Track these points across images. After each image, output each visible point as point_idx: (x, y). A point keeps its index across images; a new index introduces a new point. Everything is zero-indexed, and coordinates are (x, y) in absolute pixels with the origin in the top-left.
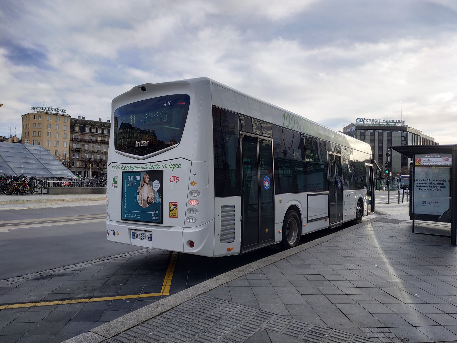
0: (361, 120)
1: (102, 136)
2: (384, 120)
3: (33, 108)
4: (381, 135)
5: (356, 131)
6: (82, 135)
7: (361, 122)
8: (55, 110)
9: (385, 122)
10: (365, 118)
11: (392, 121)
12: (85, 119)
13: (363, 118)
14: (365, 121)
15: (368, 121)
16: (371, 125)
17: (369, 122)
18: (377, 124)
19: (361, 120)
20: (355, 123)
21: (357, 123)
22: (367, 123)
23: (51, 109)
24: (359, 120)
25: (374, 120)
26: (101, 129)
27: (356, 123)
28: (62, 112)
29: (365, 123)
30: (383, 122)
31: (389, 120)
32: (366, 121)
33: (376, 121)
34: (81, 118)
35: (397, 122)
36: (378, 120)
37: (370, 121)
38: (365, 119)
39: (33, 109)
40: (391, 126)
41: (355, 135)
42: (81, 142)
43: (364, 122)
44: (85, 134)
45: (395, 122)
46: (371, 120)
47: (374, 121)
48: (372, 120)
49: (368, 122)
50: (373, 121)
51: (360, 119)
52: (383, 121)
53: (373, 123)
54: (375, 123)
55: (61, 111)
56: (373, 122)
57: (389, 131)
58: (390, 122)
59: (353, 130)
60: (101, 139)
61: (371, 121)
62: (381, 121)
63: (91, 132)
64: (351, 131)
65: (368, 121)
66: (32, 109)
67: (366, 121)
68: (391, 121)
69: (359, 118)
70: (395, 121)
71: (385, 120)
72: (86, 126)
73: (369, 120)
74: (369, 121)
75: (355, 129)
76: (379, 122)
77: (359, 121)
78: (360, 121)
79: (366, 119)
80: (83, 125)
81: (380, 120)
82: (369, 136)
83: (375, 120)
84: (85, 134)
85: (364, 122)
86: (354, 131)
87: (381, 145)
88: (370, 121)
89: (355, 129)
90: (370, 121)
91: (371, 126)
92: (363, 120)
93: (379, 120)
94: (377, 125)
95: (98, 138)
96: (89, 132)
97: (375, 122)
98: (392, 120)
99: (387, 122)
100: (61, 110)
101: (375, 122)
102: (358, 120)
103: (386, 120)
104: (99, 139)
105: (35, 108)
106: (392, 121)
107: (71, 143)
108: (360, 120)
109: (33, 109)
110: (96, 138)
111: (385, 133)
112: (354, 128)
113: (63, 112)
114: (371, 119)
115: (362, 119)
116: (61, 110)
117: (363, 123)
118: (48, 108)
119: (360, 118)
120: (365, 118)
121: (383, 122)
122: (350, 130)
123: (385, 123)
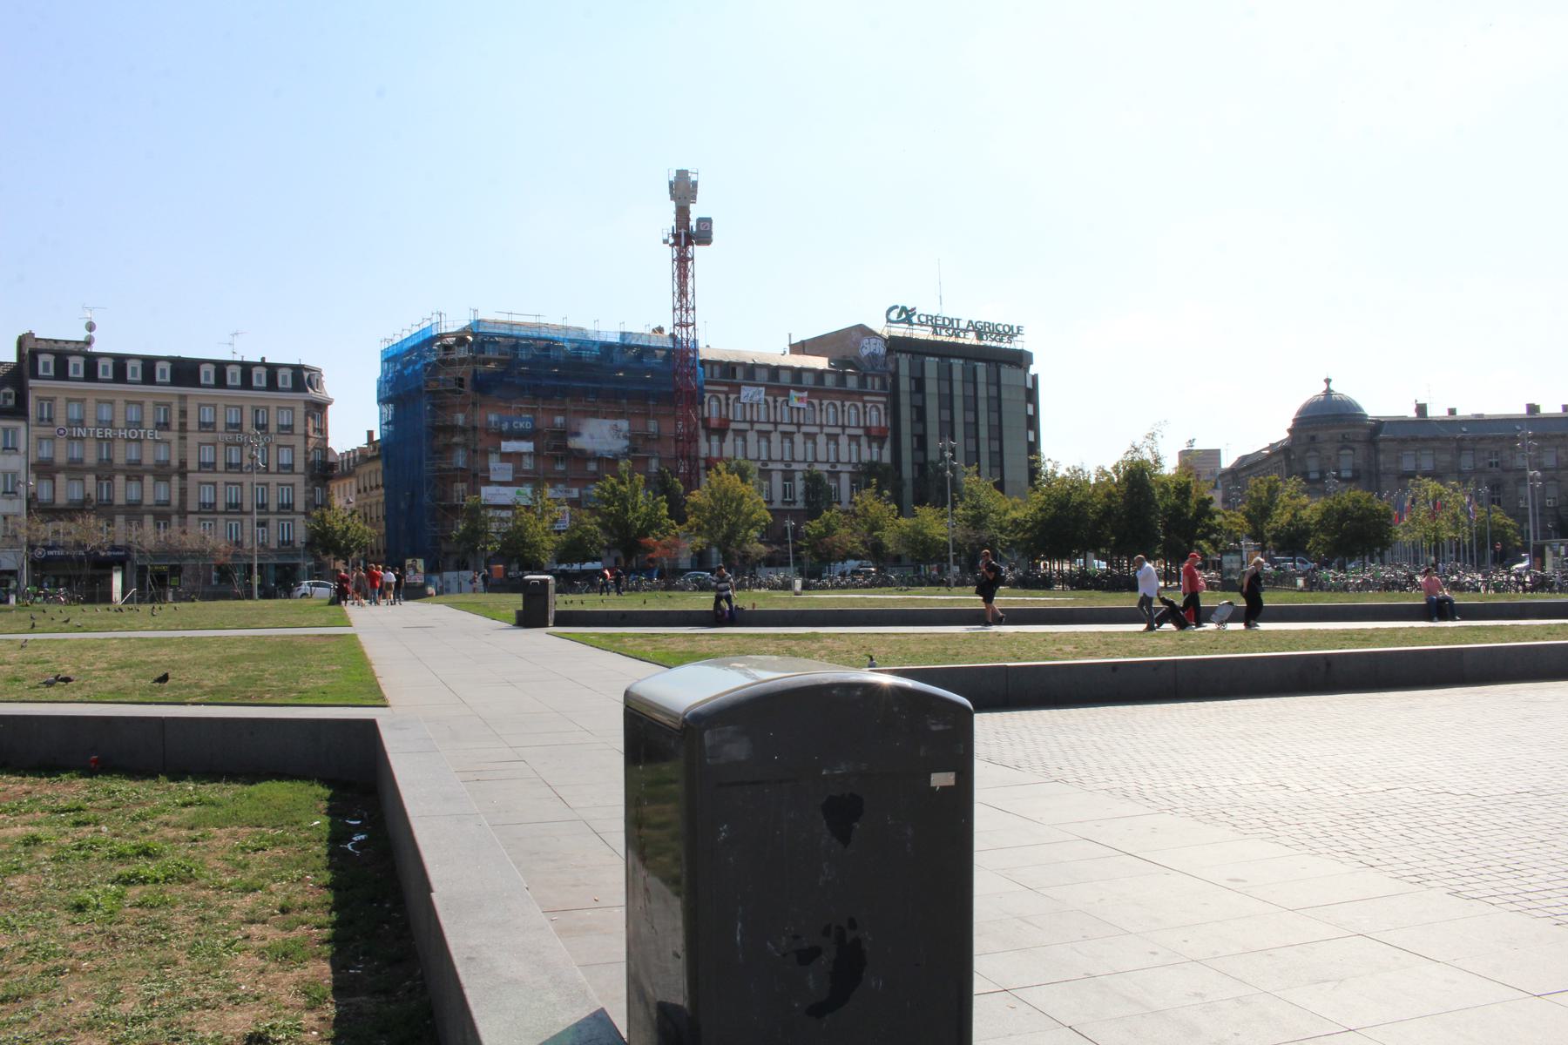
0: (904, 316)
7: (902, 321)
10: (915, 309)
11: (991, 328)
15: (923, 319)
19: (904, 316)
24: (896, 315)
29: (915, 327)
30: (966, 331)
31: (985, 323)
35: (1006, 334)
37: (931, 320)
38: (915, 314)
43: (911, 323)
45: (999, 333)
46: (932, 316)
47: (940, 322)
48: (936, 317)
49: (921, 324)
52: (968, 326)
54: (943, 332)
58: (987, 329)
61: (934, 321)
68: (989, 327)
69: (896, 307)
70: (1000, 328)
73: (927, 316)
74: (927, 320)
79: (918, 313)
81: (958, 320)
82: (936, 381)
83: (944, 318)
85: (911, 323)
88: (930, 323)
90: (930, 323)
92: (907, 315)
93: (955, 322)
102: (894, 316)
106: (991, 328)
108: (900, 315)
115: (904, 309)
117: (906, 326)
120: (915, 309)
121: (966, 331)
123: (970, 339)
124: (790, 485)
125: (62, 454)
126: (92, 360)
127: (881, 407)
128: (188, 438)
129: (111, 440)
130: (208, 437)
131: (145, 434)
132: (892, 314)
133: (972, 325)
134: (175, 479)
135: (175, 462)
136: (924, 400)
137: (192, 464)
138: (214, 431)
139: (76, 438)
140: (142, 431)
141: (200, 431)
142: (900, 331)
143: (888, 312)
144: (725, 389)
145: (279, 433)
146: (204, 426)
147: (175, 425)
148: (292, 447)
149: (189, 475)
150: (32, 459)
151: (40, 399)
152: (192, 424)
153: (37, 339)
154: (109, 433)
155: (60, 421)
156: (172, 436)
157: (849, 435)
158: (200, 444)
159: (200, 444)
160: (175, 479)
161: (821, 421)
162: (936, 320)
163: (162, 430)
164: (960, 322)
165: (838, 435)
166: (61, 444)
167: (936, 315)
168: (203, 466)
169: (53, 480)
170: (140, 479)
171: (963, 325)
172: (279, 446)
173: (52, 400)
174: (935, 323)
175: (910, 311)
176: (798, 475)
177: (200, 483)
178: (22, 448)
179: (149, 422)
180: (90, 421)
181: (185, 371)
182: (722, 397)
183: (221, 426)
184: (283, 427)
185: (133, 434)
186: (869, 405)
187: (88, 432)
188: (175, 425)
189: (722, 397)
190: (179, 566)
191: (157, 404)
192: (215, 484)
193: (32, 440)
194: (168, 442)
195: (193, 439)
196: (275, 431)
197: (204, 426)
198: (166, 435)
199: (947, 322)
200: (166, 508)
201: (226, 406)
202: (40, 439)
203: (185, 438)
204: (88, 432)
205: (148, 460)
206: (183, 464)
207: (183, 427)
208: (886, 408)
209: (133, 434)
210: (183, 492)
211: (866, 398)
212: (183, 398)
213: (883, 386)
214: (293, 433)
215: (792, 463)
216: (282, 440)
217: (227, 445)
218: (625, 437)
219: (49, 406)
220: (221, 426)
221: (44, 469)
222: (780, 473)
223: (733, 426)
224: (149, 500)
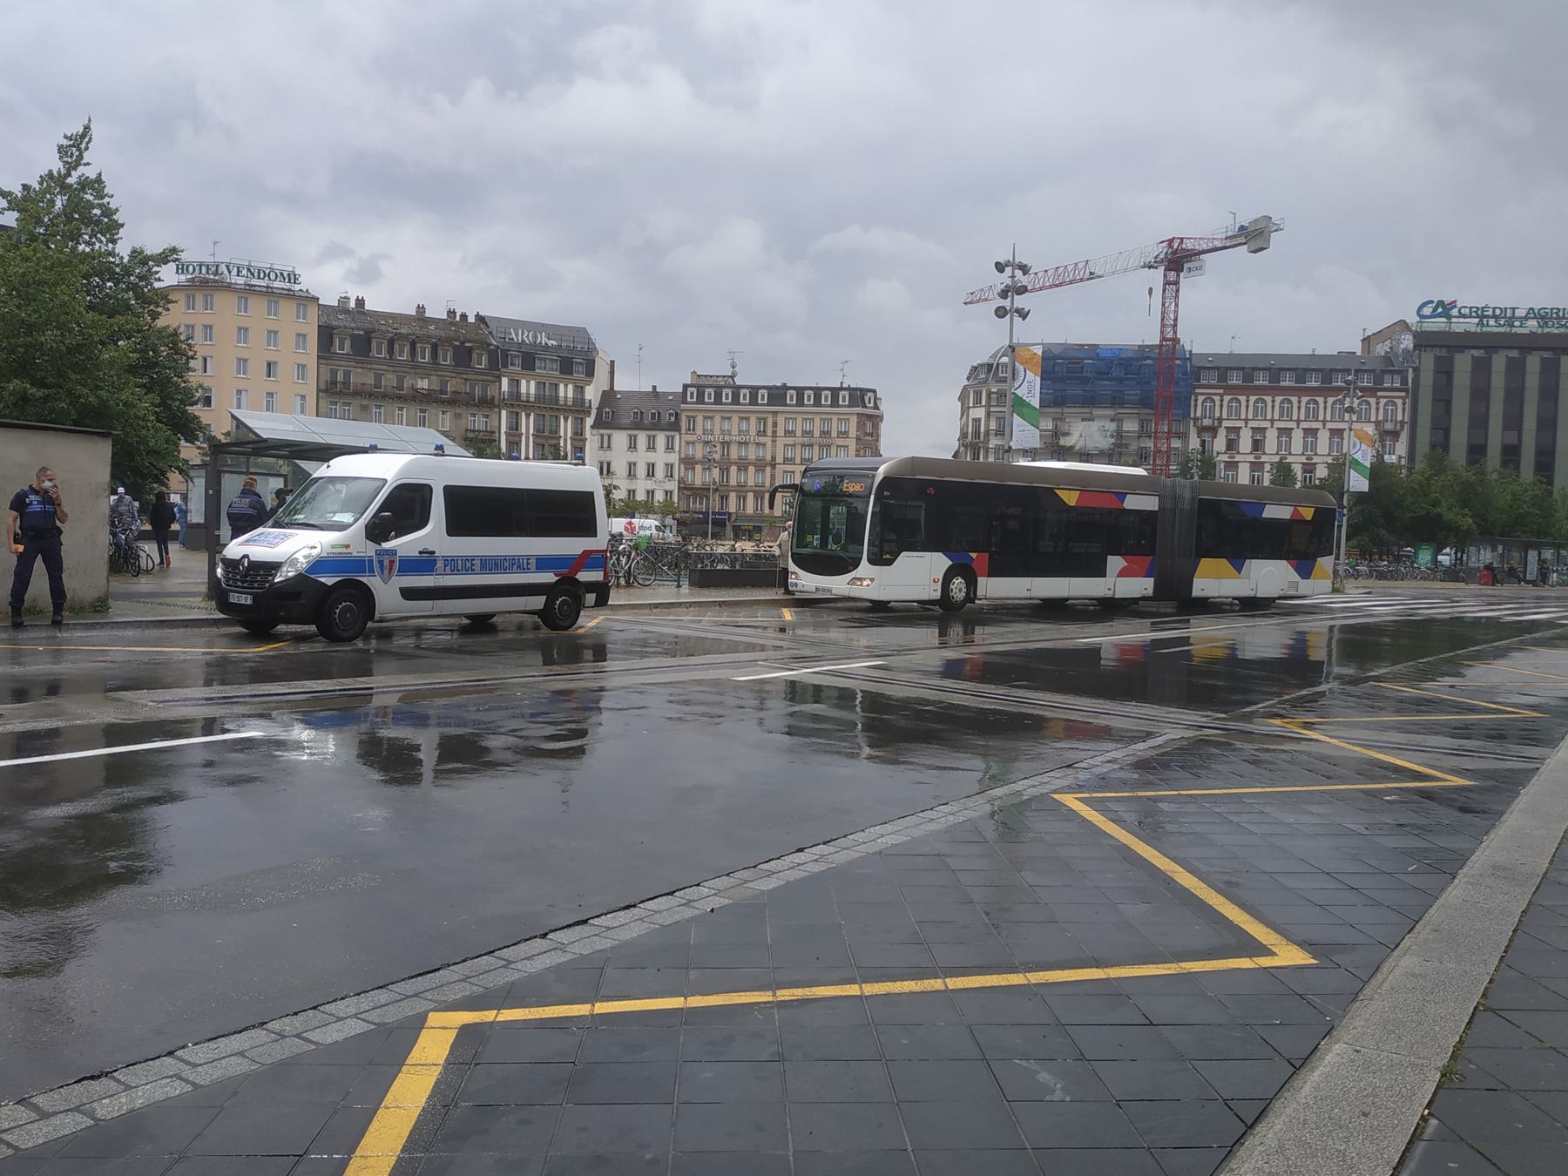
0: (1440, 310)
1: (433, 372)
2: (1531, 309)
3: (182, 269)
4: (1516, 369)
5: (1418, 352)
6: (360, 370)
7: (1439, 315)
8: (262, 275)
9: (1535, 318)
10: (1455, 301)
11: (1561, 314)
12: (366, 308)
13: (1447, 300)
14: (1455, 312)
16: (1479, 330)
17: (1470, 317)
18: (1500, 324)
19: (1440, 310)
20: (1412, 319)
21: (1423, 320)
22: (1462, 320)
23: (249, 270)
24: (1431, 309)
25: (1491, 310)
26: (430, 346)
27: (1418, 319)
28: (287, 280)
29: (1454, 320)
30: (1526, 318)
31: (1552, 309)
32: (1457, 314)
33: (1498, 312)
34: (352, 304)
36: (1506, 309)
38: (1455, 307)
39: (180, 271)
40: (1556, 331)
41: (1411, 370)
42: (359, 397)
43: (1449, 317)
44: (369, 366)
47: (1490, 313)
49: (1464, 316)
50: (1485, 313)
51: (1434, 305)
52: (1528, 313)
53: (1485, 322)
54: (1492, 322)
55: (284, 279)
56: (1487, 316)
57: (1547, 354)
58: (1554, 315)
59: (1402, 346)
60: (429, 386)
61: (1479, 312)
62: (1518, 313)
63: (391, 358)
64: (1397, 355)
65: (1467, 311)
66: (177, 273)
67: (1457, 314)
69: (1432, 302)
71: (1536, 311)
72: (373, 335)
73: (1471, 308)
74: (1471, 312)
75: (1415, 346)
76: (1508, 315)
77: (1428, 314)
78: (1433, 312)
80: (362, 333)
81: (1514, 309)
83: (1494, 309)
84: (369, 366)
86: (1406, 351)
88: (1474, 314)
89: (1412, 346)
90: (1474, 314)
91: (1475, 333)
92: (1444, 309)
93: (1508, 311)
94: (1502, 330)
95: (419, 381)
96: (385, 358)
97: (1495, 316)
98: (1561, 307)
99: (1542, 318)
100: (282, 274)
101: (1495, 316)
102: (1427, 311)
103: (1537, 307)
104: (423, 384)
105: (191, 268)
107: (320, 401)
108: (1435, 309)
109: (180, 271)
110: (411, 382)
111: (1533, 363)
112: (1407, 342)
113: (289, 281)
114: (1480, 306)
115: (1441, 303)
116: (285, 275)
117: (1444, 320)
118: (238, 268)
119: (1436, 300)
120: (1455, 301)
121: (1526, 318)
122: (1390, 348)
124: (1233, 475)
125: (699, 452)
126: (737, 390)
127: (1399, 402)
128: (777, 443)
129: (728, 443)
130: (790, 441)
131: (750, 439)
132: (1424, 309)
133: (1534, 313)
134: (768, 469)
135: (769, 458)
136: (1451, 391)
137: (779, 459)
138: (795, 436)
139: (708, 442)
140: (748, 437)
141: (785, 436)
142: (1438, 324)
143: (1420, 308)
144: (1221, 391)
145: (838, 437)
146: (789, 433)
147: (769, 433)
148: (847, 446)
149: (777, 466)
150: (683, 456)
151: (688, 417)
152: (780, 432)
153: (699, 376)
154: (727, 438)
155: (699, 430)
156: (768, 440)
158: (785, 445)
159: (785, 445)
160: (768, 469)
161: (1299, 417)
162: (1483, 311)
163: (761, 436)
164: (1516, 311)
165: (1317, 430)
166: (699, 447)
167: (1484, 305)
168: (786, 461)
169: (694, 468)
170: (746, 470)
171: (1520, 313)
172: (838, 446)
173: (694, 417)
174: (1480, 314)
175: (1448, 304)
176: (1267, 467)
177: (785, 472)
178: (677, 448)
179: (753, 432)
180: (717, 431)
181: (777, 395)
182: (1217, 399)
183: (799, 433)
184: (840, 433)
185: (742, 439)
186: (1383, 401)
187: (715, 438)
188: (769, 433)
189: (1217, 399)
190: (760, 527)
191: (759, 419)
192: (793, 472)
193: (683, 444)
194: (764, 445)
195: (780, 442)
196: (836, 436)
197: (789, 433)
198: (762, 439)
199: (1498, 312)
200: (762, 489)
201: (803, 419)
202: (688, 443)
203: (775, 441)
204: (715, 438)
205: (752, 457)
206: (774, 458)
207: (774, 432)
208: (1404, 404)
209: (742, 439)
210: (773, 477)
211: (1379, 394)
212: (775, 413)
213: (1404, 381)
214: (848, 437)
215: (1313, 457)
216: (840, 442)
217: (803, 445)
218: (1112, 436)
219: (694, 421)
220: (799, 433)
221: (689, 463)
222: (1301, 466)
223: (1226, 424)
224: (751, 483)
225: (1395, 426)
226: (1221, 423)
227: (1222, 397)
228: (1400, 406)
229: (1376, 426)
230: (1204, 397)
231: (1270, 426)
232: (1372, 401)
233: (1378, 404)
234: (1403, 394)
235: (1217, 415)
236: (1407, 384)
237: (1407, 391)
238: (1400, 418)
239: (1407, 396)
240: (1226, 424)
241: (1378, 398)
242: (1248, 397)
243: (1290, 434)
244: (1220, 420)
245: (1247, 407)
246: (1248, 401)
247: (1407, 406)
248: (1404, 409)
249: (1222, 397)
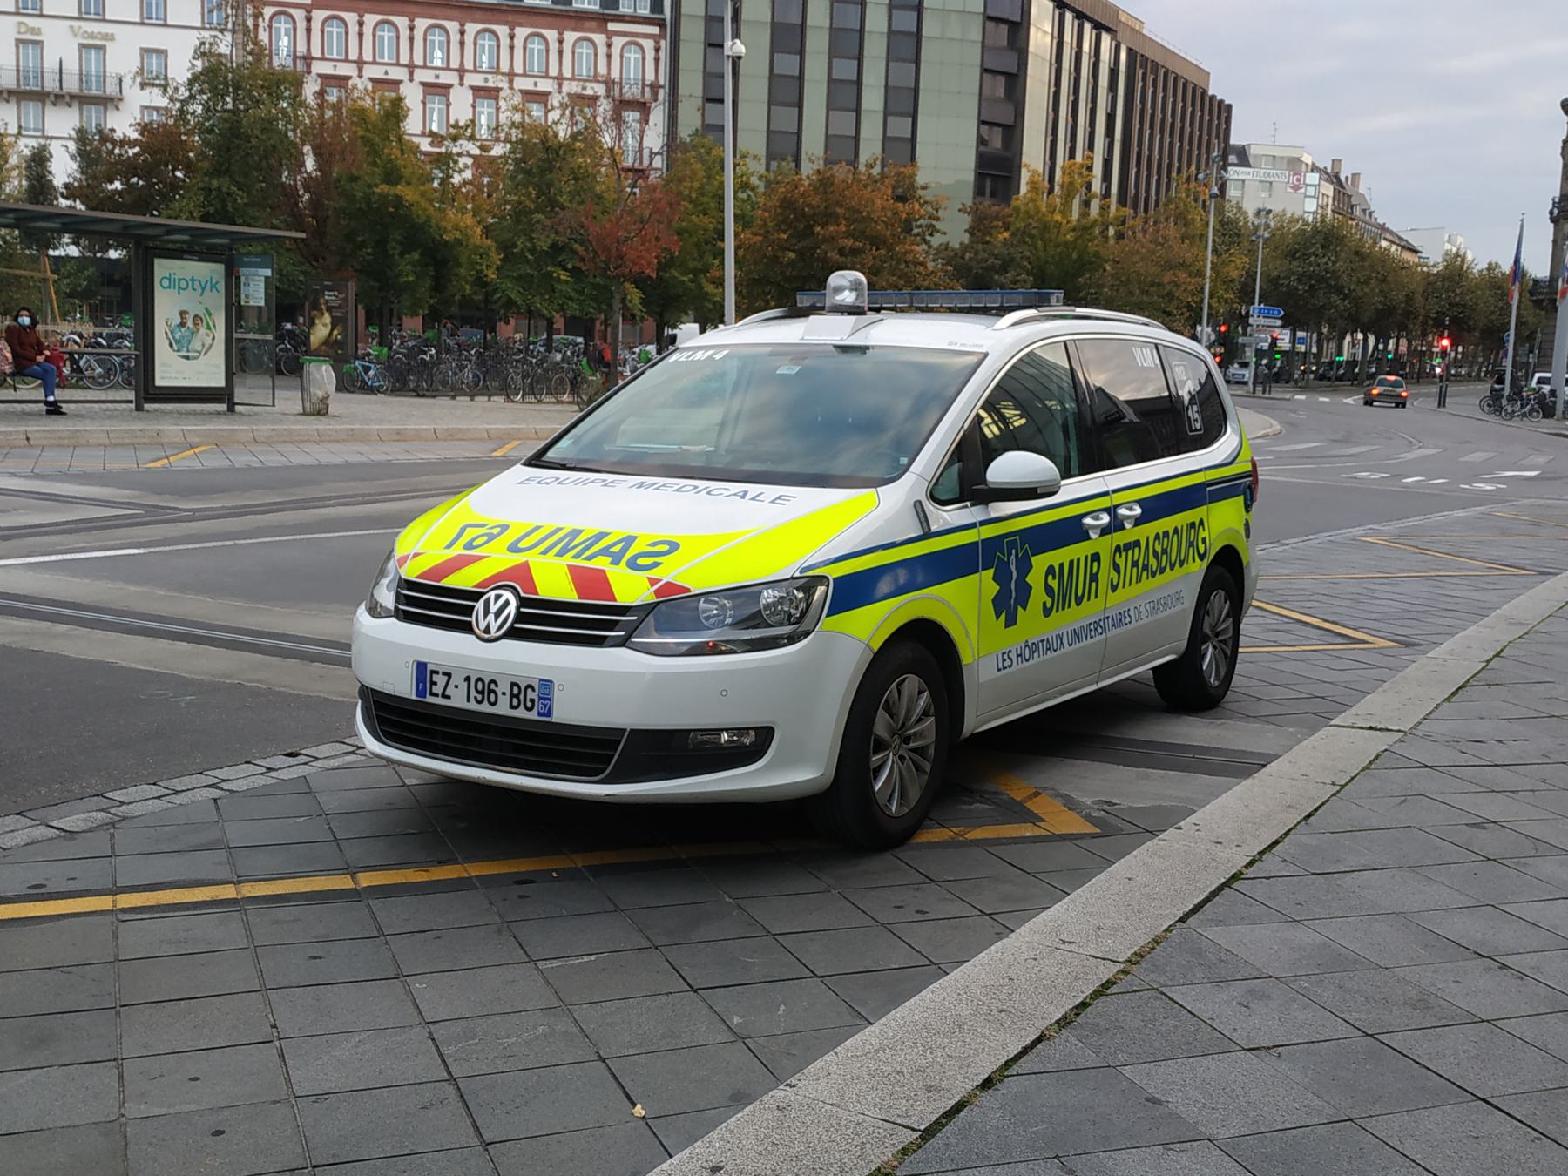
87: (846, 70)
127: (648, 45)
157: (473, 88)
186: (618, 42)
208: (657, 50)
211: (612, 26)
223: (319, 68)
225: (643, 92)
226: (309, 66)
227: (309, 12)
228: (650, 55)
229: (608, 90)
230: (274, 9)
231: (357, 73)
232: (599, 39)
233: (609, 46)
234: (655, 30)
235: (301, 49)
236: (661, 12)
237: (661, 24)
238: (650, 77)
239: (662, 35)
240: (319, 68)
241: (610, 35)
242: (361, 16)
243: (447, 96)
244: (308, 59)
245: (361, 35)
246: (361, 24)
247: (662, 54)
248: (657, 60)
249: (309, 12)
